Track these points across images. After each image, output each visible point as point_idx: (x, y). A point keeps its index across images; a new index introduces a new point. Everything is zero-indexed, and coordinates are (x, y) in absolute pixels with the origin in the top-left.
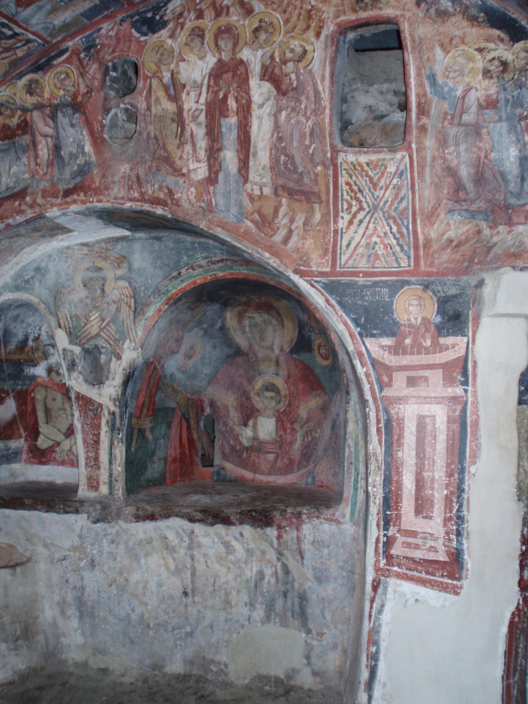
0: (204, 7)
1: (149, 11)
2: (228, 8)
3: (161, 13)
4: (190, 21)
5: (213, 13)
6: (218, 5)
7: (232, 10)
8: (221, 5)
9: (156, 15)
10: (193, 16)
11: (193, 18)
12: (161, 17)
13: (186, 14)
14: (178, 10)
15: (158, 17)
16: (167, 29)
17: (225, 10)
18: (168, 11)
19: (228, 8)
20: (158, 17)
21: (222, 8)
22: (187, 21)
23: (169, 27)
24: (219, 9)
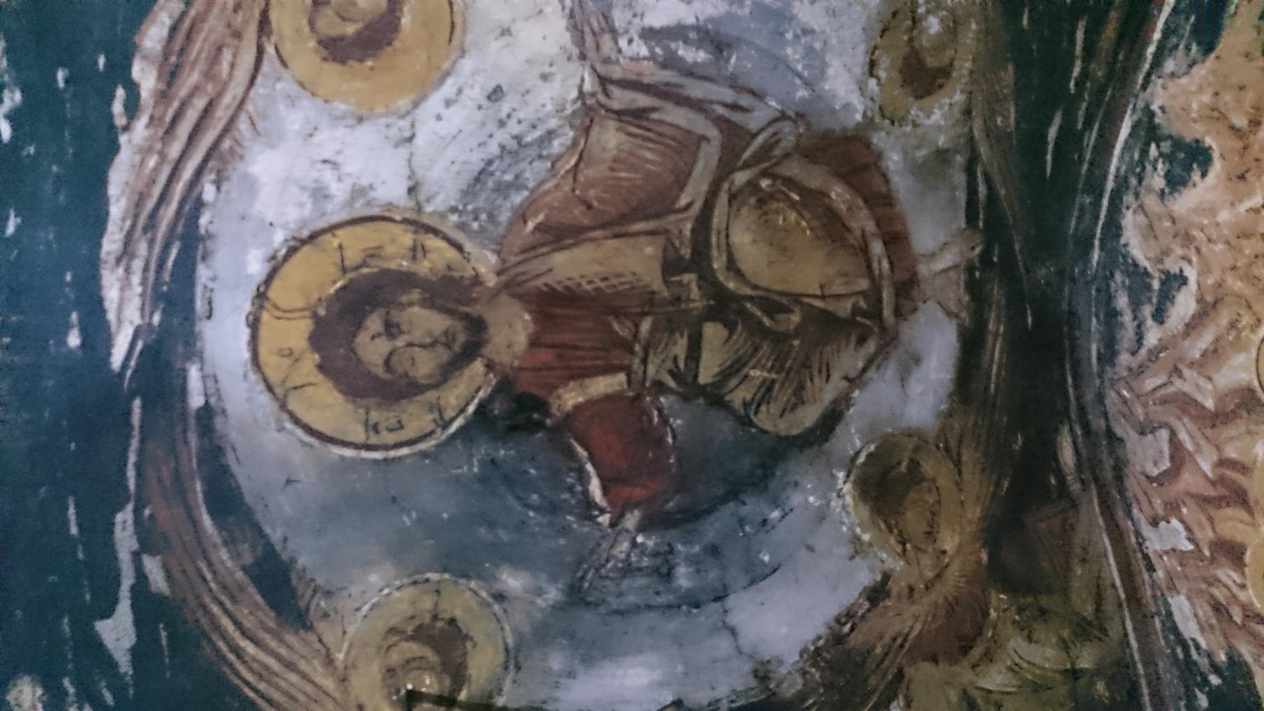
0: (1211, 535)
1: (1191, 698)
2: (1223, 463)
3: (1204, 662)
4: (1243, 587)
5: (1229, 512)
6: (1211, 492)
7: (1231, 453)
8: (1213, 483)
9: (1206, 681)
10: (1227, 574)
11: (1235, 576)
12: (1216, 669)
13: (1219, 593)
14: (1205, 611)
15: (1215, 680)
16: (1255, 668)
17: (1228, 473)
18: (1203, 644)
19: (1223, 463)
20: (1215, 680)
21: (1221, 481)
22: (1242, 596)
23: (1249, 659)
24: (1222, 491)
